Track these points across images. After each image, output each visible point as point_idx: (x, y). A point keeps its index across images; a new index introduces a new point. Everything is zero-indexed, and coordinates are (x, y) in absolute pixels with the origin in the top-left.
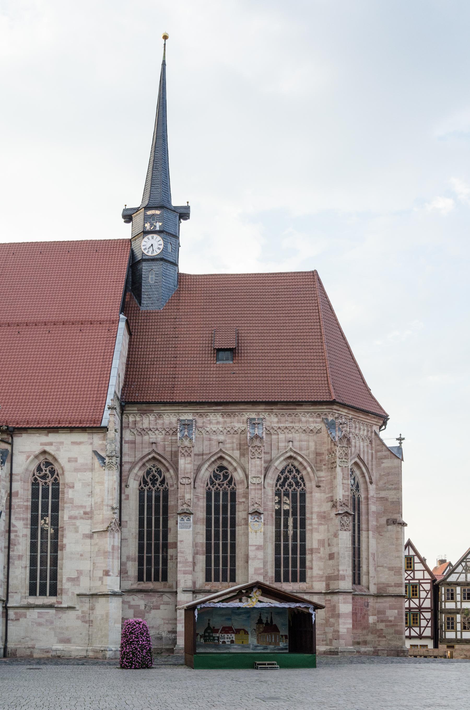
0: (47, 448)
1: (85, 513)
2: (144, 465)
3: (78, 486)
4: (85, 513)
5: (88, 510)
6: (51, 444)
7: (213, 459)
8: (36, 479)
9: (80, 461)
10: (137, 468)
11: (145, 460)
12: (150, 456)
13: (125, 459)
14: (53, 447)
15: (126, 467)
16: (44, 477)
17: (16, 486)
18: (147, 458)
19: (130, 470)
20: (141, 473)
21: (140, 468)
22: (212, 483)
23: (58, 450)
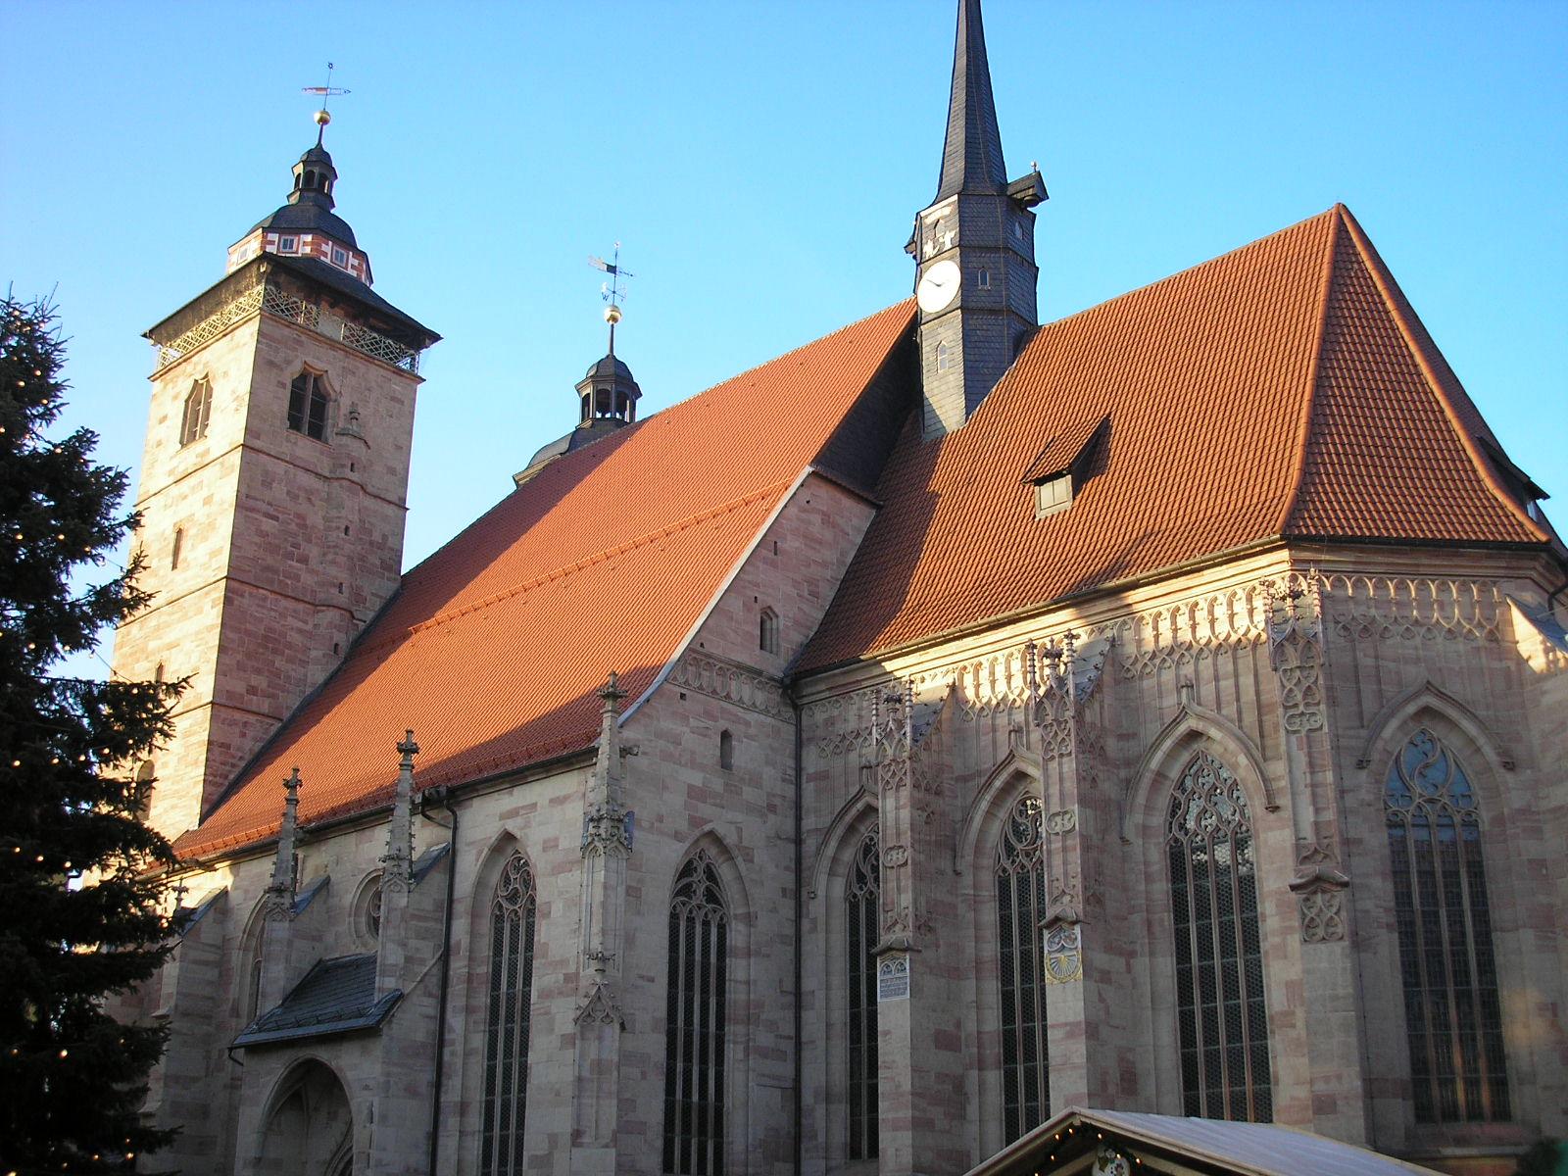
0: (512, 826)
1: (568, 978)
2: (852, 829)
3: (557, 909)
4: (568, 978)
5: (572, 969)
6: (513, 813)
7: (998, 783)
8: (501, 906)
9: (563, 844)
10: (833, 844)
11: (848, 818)
12: (860, 805)
13: (809, 822)
14: (519, 821)
15: (810, 844)
16: (513, 898)
17: (460, 927)
18: (853, 812)
19: (819, 852)
20: (848, 855)
21: (843, 842)
22: (1010, 849)
23: (527, 825)
